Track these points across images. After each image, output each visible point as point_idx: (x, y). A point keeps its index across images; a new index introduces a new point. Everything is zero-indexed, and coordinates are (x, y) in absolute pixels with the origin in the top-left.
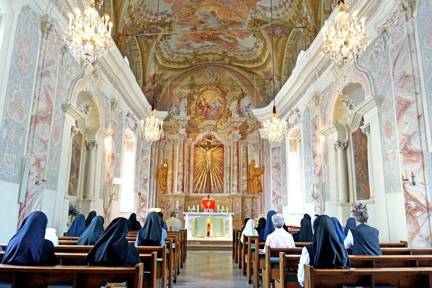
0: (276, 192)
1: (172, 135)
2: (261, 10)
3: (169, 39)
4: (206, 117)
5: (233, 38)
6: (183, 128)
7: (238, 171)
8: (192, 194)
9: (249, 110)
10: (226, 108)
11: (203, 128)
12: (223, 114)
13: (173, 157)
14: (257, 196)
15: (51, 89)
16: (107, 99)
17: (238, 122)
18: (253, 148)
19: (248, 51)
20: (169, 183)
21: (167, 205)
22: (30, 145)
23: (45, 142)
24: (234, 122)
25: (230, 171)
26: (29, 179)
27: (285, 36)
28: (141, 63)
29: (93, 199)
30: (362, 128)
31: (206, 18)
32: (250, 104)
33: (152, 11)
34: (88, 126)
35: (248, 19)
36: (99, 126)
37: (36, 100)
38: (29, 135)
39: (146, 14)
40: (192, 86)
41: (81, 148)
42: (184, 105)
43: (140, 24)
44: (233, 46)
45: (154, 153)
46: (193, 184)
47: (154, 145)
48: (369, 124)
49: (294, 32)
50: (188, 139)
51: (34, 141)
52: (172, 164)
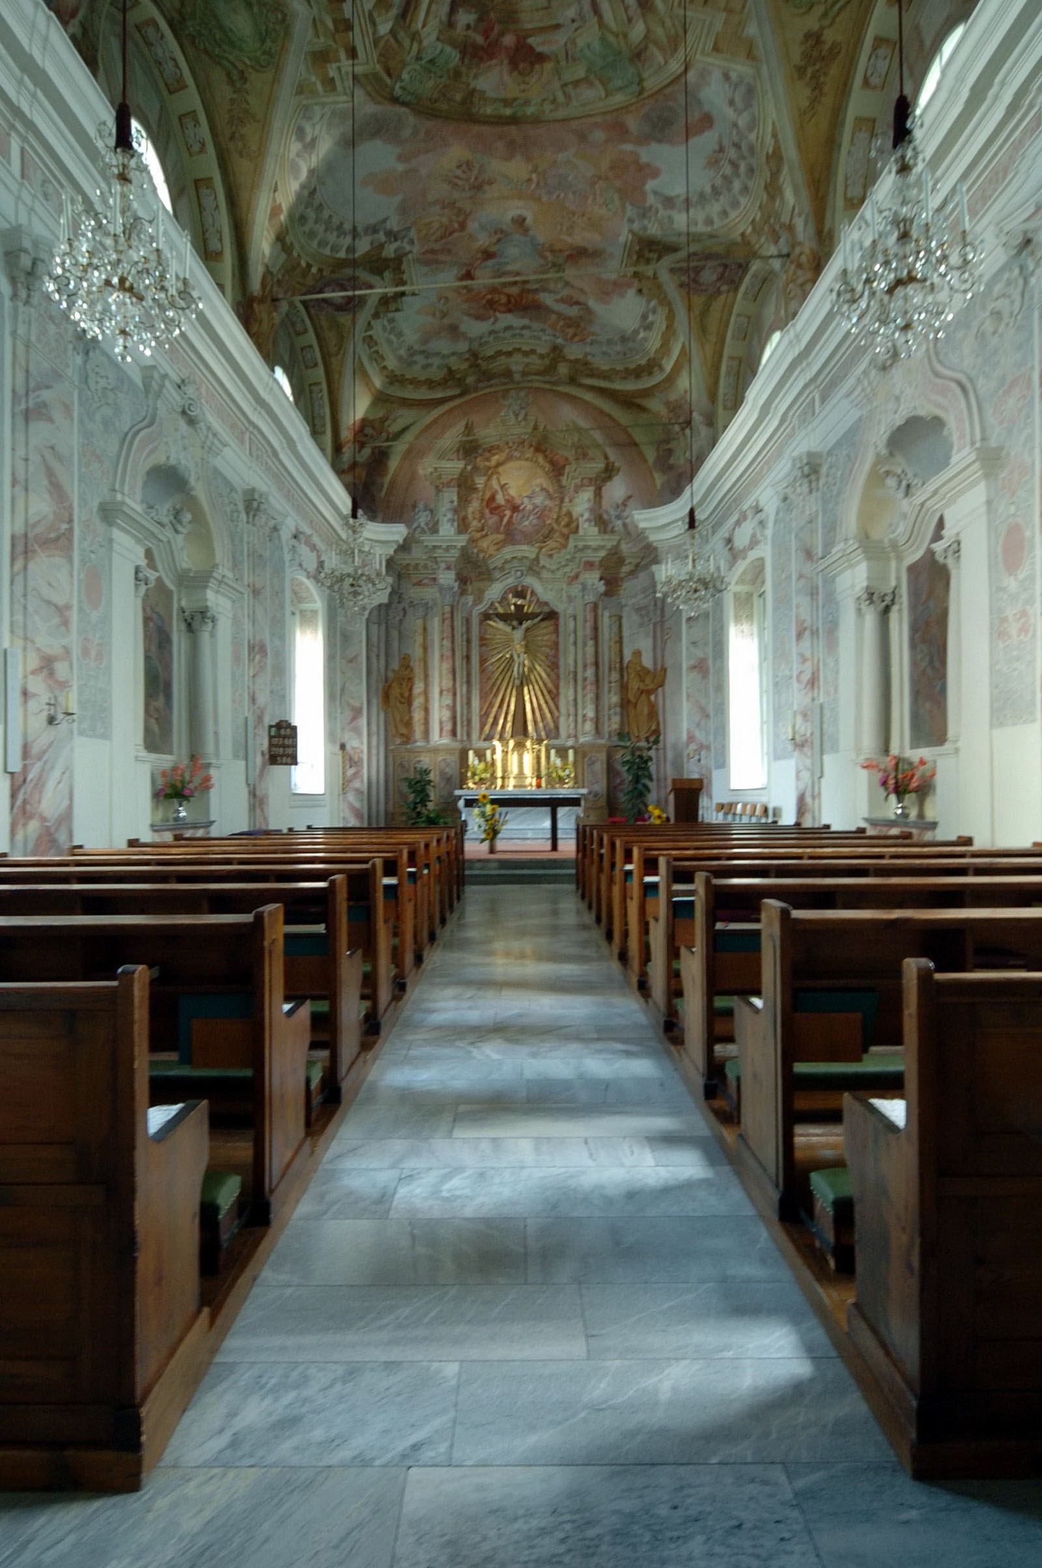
0: (697, 734)
1: (419, 589)
2: (660, 206)
3: (397, 310)
4: (510, 536)
5: (578, 303)
6: (448, 568)
7: (597, 681)
9: (625, 514)
10: (564, 510)
11: (502, 569)
12: (556, 527)
13: (425, 648)
15: (59, 457)
16: (233, 490)
17: (596, 549)
18: (635, 618)
19: (624, 339)
20: (418, 716)
22: (19, 617)
23: (62, 611)
24: (586, 547)
25: (576, 681)
26: (25, 710)
27: (729, 291)
28: (324, 386)
29: (214, 761)
30: (938, 547)
31: (499, 241)
32: (630, 497)
33: (342, 224)
34: (185, 566)
35: (622, 239)
36: (216, 566)
37: (19, 489)
38: (12, 590)
39: (326, 230)
40: (470, 449)
41: (171, 625)
42: (449, 506)
43: (309, 266)
44: (579, 325)
45: (375, 639)
46: (481, 717)
47: (374, 619)
48: (958, 534)
49: (755, 276)
50: (463, 600)
51: (30, 609)
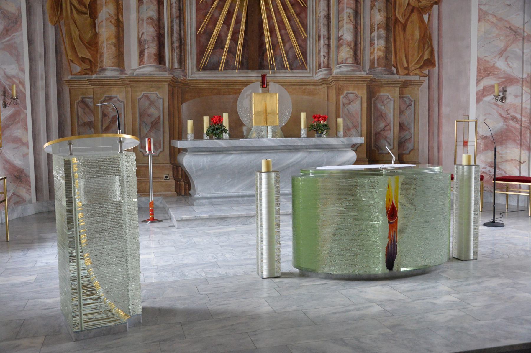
0: (501, 64)
8: (195, 75)
14: (417, 78)
20: (106, 32)
21: (104, 115)
46: (198, 36)
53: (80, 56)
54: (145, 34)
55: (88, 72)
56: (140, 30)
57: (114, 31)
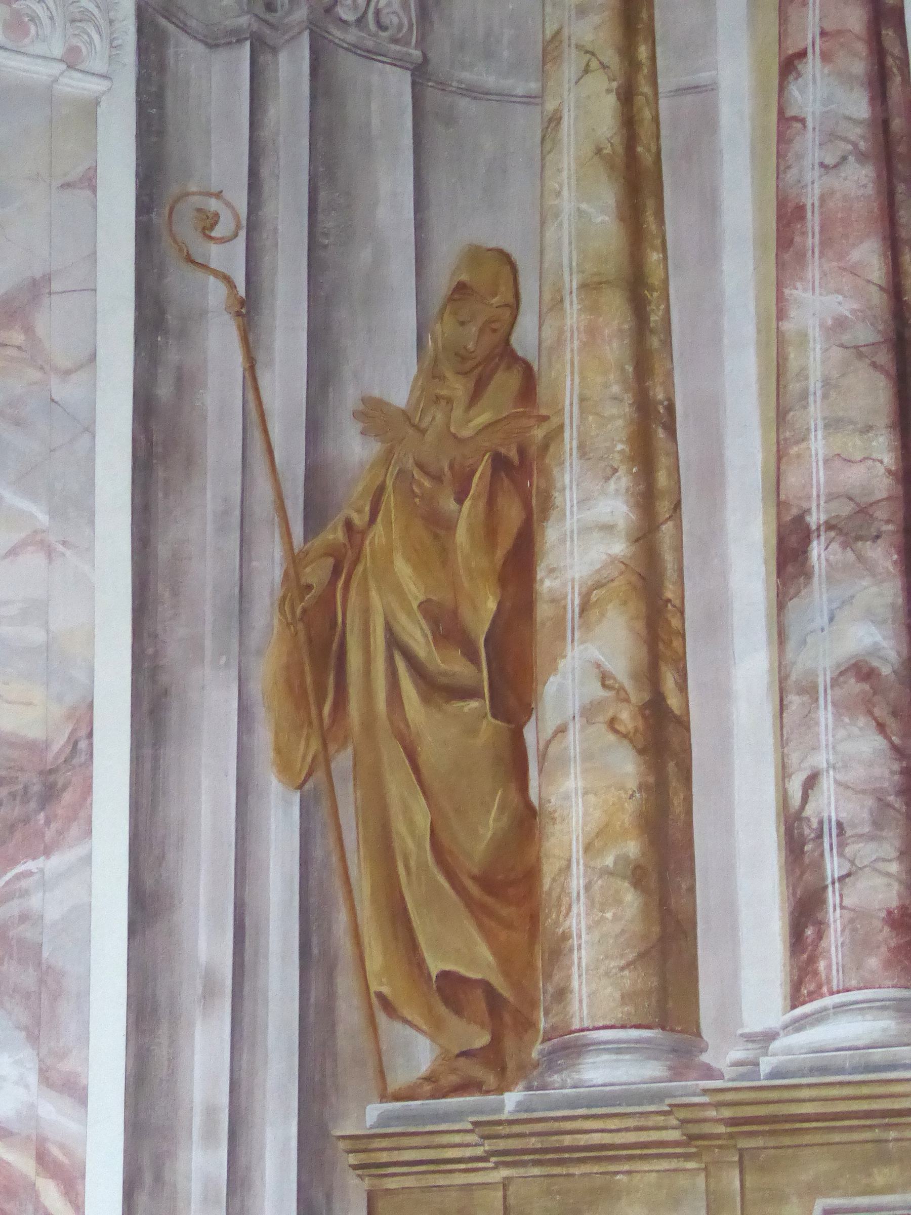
13: (638, 180)
20: (584, 794)
45: (218, 165)
52: (615, 350)
53: (435, 966)
54: (827, 784)
55: (476, 1071)
56: (794, 758)
57: (632, 784)
